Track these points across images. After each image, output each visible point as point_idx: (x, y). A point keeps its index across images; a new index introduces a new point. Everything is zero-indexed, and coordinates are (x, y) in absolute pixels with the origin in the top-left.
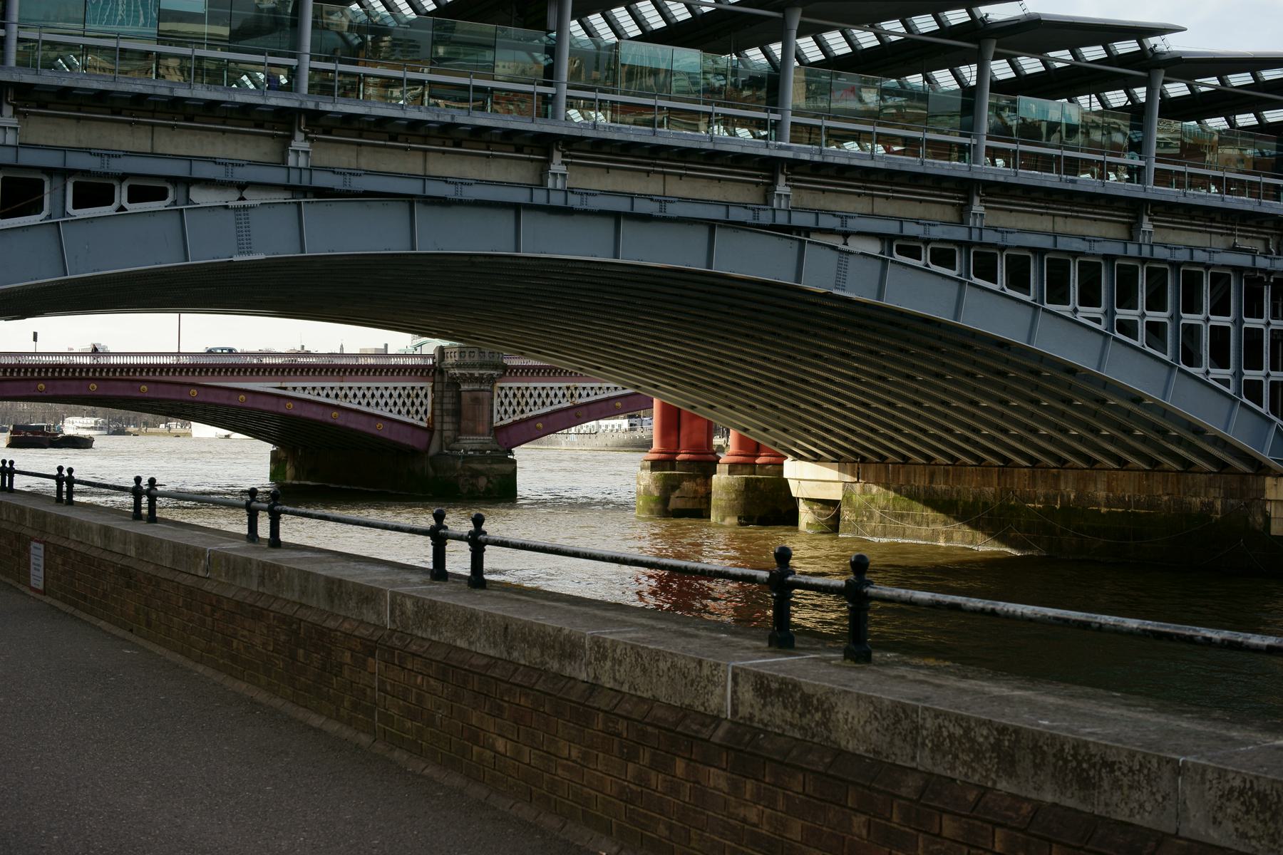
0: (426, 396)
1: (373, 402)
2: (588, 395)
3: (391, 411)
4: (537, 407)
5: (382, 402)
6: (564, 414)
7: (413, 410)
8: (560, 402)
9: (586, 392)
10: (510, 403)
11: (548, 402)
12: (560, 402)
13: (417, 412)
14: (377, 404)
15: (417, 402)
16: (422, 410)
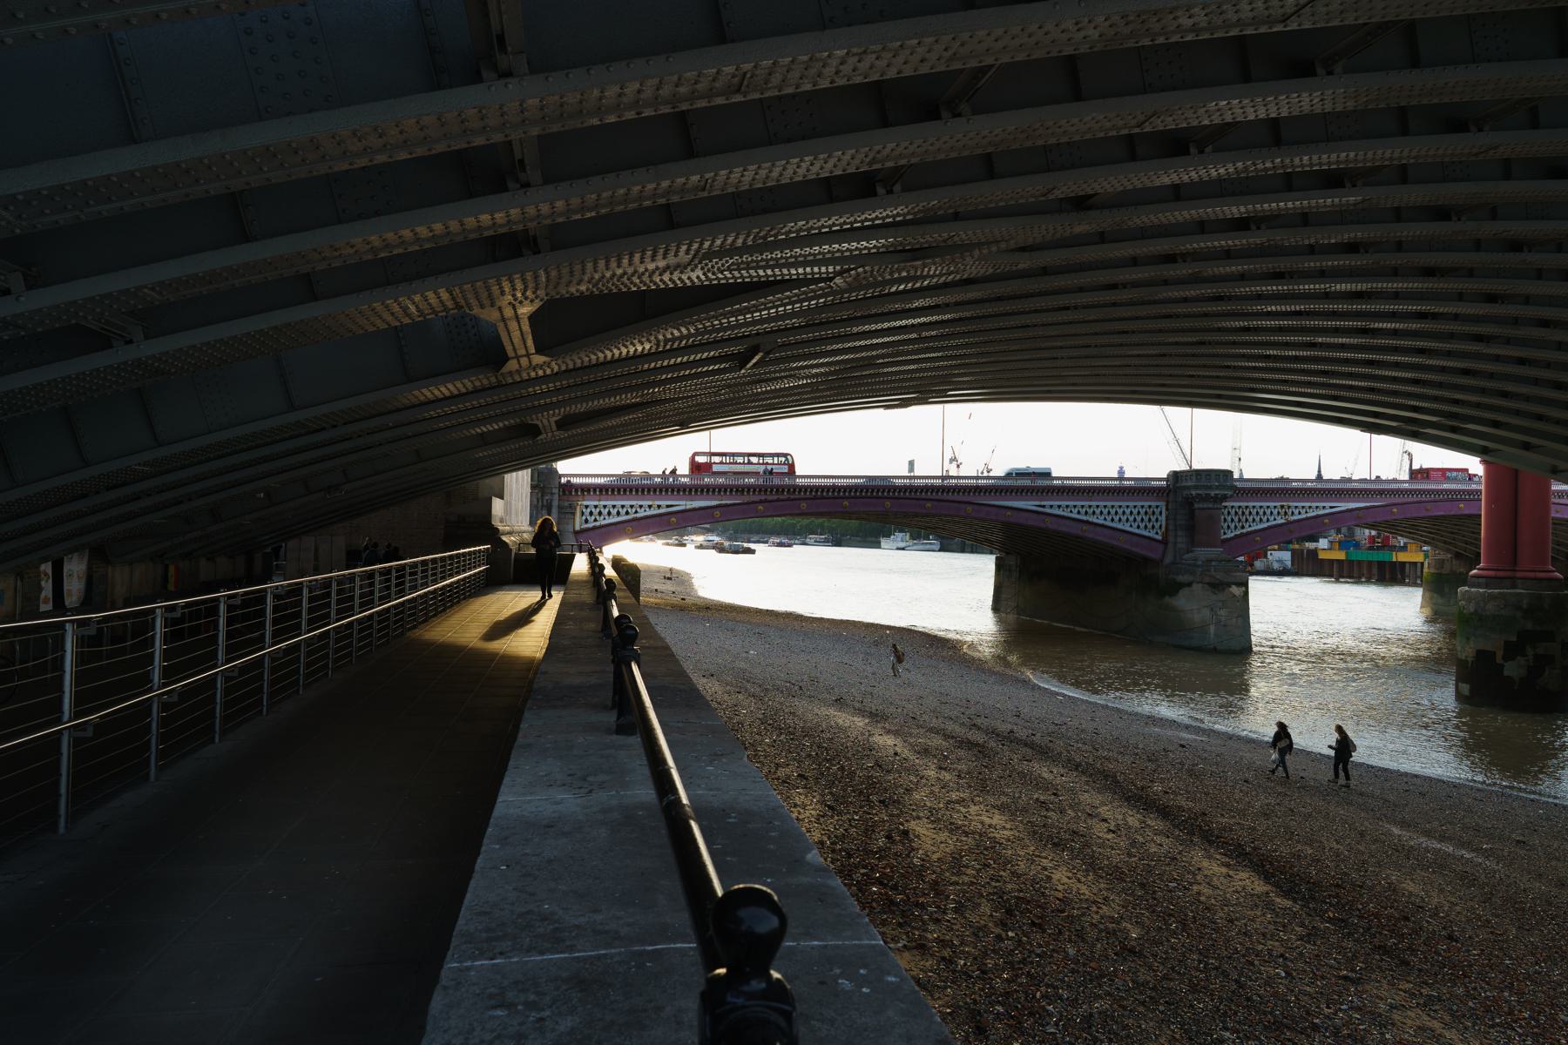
0: (1161, 513)
1: (1116, 519)
2: (1300, 513)
3: (1131, 526)
4: (602, 517)
5: (1124, 518)
6: (658, 519)
7: (1150, 526)
8: (1275, 519)
9: (1297, 511)
10: (1232, 520)
11: (1265, 519)
12: (1275, 519)
13: (1153, 527)
14: (1120, 520)
15: (1153, 519)
16: (1157, 525)
